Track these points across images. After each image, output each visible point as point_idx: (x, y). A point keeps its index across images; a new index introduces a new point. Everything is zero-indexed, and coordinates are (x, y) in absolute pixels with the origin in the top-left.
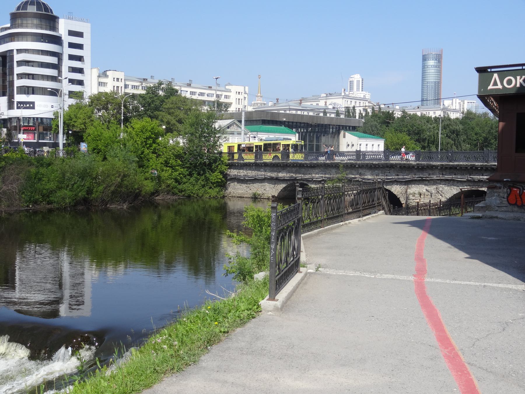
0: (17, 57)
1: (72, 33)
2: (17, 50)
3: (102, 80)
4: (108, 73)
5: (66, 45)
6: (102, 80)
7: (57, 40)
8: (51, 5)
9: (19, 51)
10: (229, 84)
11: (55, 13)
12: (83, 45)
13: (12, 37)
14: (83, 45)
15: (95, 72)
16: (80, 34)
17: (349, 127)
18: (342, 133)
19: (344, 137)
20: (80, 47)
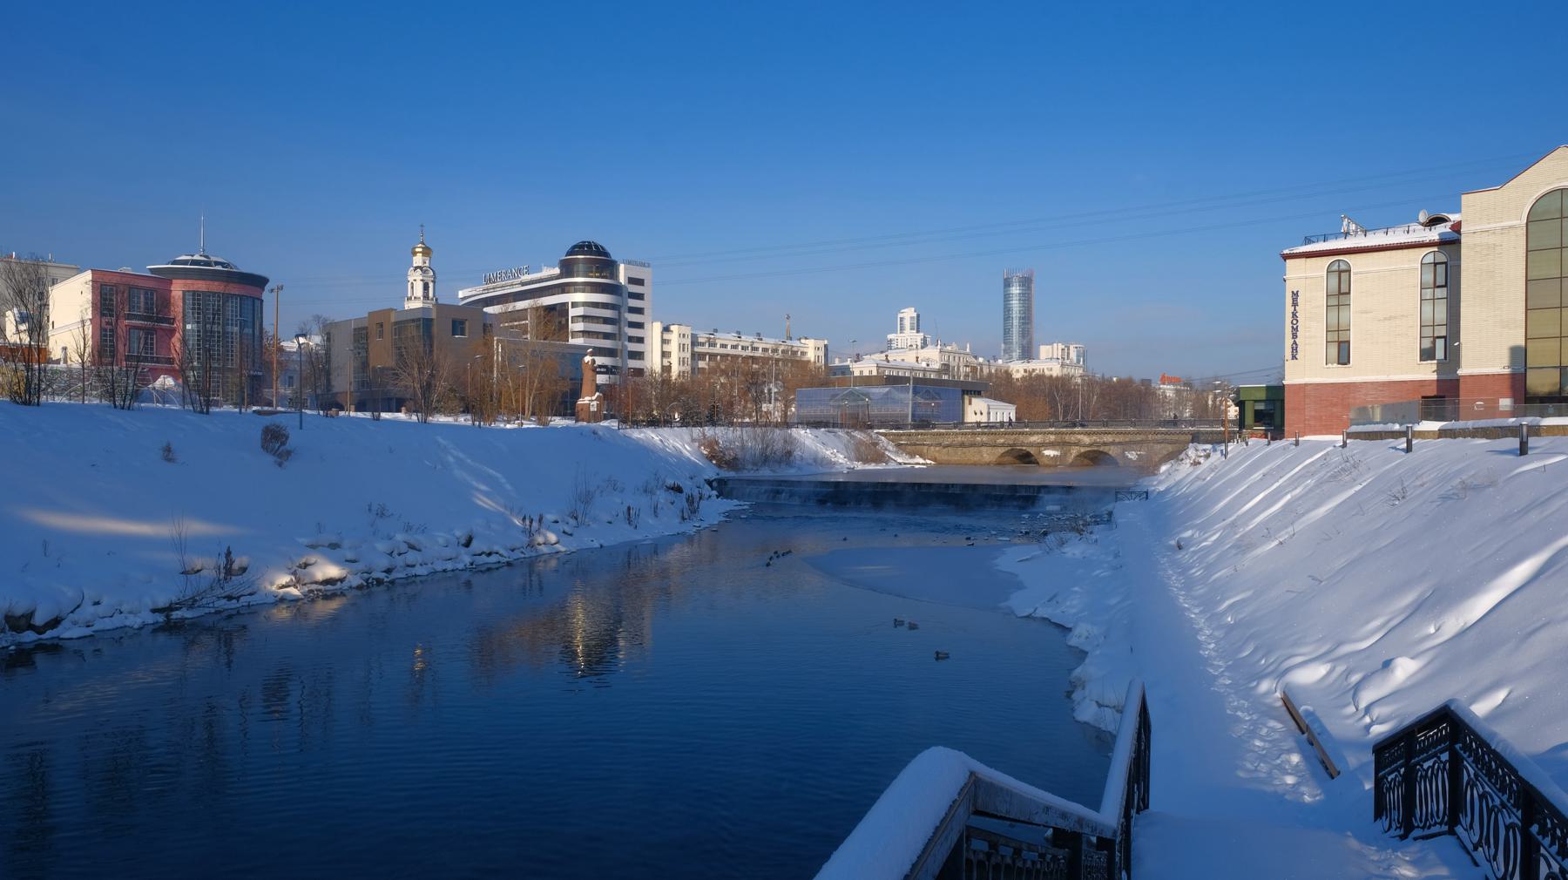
0: (572, 312)
1: (632, 281)
2: (572, 303)
3: (666, 336)
4: (672, 328)
5: (625, 295)
6: (666, 336)
7: (614, 289)
8: (609, 249)
9: (575, 305)
10: (806, 338)
11: (614, 257)
12: (643, 294)
13: (563, 289)
14: (643, 294)
15: (657, 327)
16: (640, 282)
17: (975, 392)
18: (966, 397)
19: (970, 403)
20: (640, 297)
